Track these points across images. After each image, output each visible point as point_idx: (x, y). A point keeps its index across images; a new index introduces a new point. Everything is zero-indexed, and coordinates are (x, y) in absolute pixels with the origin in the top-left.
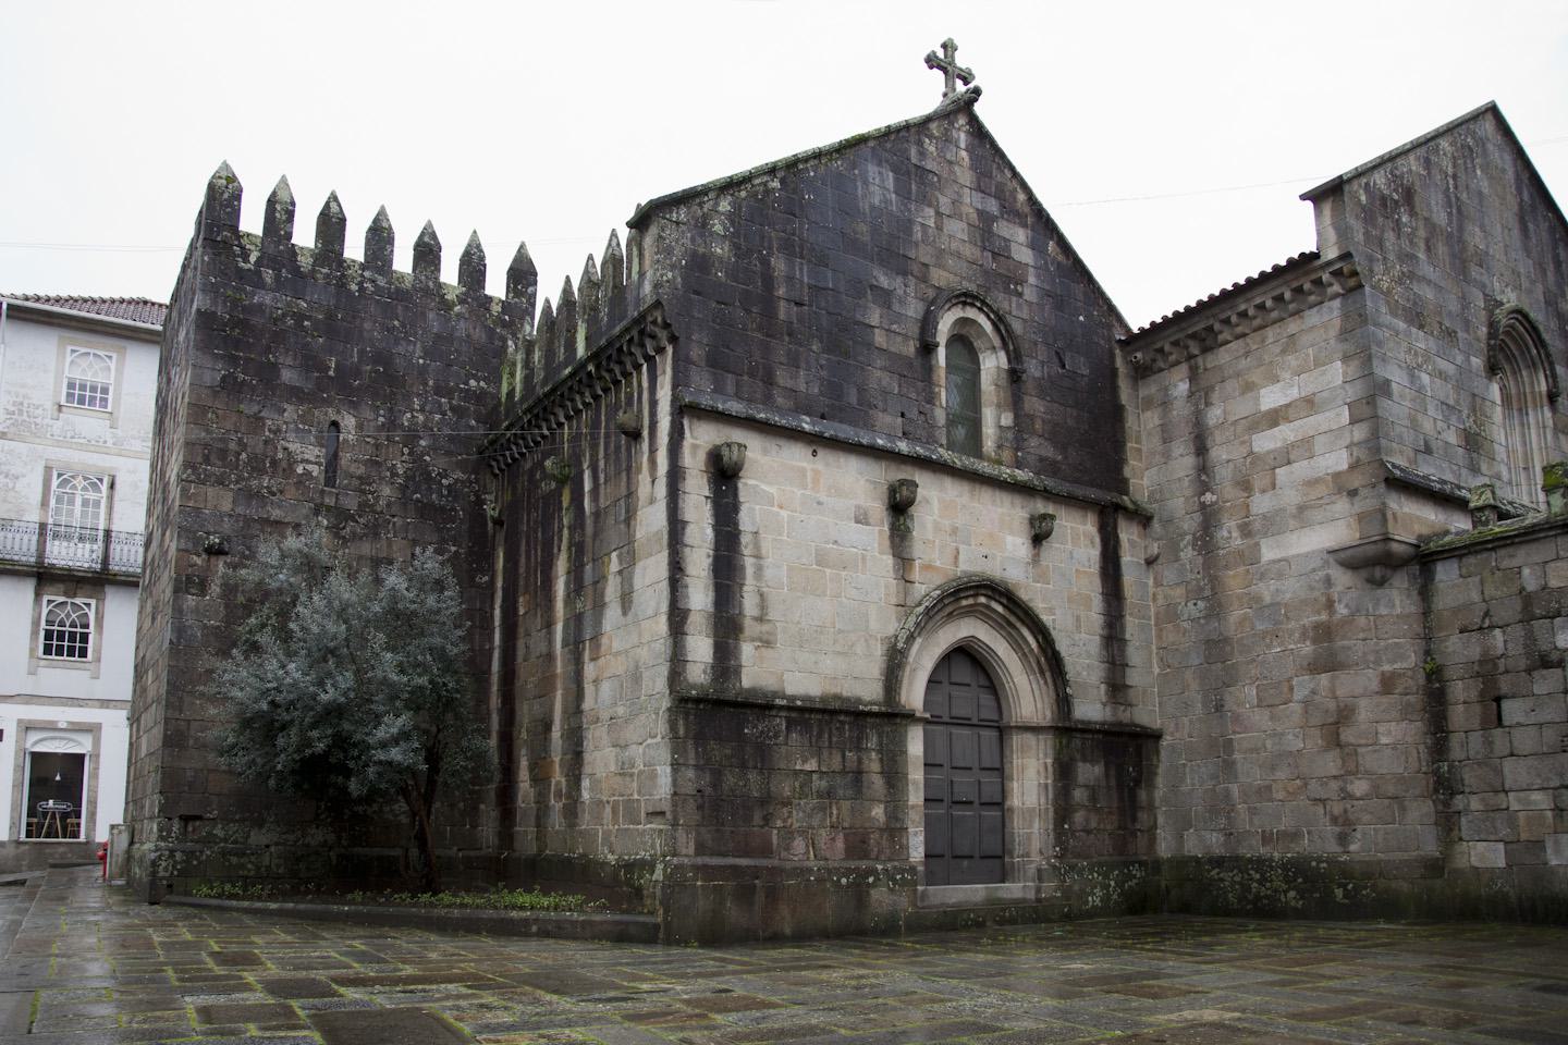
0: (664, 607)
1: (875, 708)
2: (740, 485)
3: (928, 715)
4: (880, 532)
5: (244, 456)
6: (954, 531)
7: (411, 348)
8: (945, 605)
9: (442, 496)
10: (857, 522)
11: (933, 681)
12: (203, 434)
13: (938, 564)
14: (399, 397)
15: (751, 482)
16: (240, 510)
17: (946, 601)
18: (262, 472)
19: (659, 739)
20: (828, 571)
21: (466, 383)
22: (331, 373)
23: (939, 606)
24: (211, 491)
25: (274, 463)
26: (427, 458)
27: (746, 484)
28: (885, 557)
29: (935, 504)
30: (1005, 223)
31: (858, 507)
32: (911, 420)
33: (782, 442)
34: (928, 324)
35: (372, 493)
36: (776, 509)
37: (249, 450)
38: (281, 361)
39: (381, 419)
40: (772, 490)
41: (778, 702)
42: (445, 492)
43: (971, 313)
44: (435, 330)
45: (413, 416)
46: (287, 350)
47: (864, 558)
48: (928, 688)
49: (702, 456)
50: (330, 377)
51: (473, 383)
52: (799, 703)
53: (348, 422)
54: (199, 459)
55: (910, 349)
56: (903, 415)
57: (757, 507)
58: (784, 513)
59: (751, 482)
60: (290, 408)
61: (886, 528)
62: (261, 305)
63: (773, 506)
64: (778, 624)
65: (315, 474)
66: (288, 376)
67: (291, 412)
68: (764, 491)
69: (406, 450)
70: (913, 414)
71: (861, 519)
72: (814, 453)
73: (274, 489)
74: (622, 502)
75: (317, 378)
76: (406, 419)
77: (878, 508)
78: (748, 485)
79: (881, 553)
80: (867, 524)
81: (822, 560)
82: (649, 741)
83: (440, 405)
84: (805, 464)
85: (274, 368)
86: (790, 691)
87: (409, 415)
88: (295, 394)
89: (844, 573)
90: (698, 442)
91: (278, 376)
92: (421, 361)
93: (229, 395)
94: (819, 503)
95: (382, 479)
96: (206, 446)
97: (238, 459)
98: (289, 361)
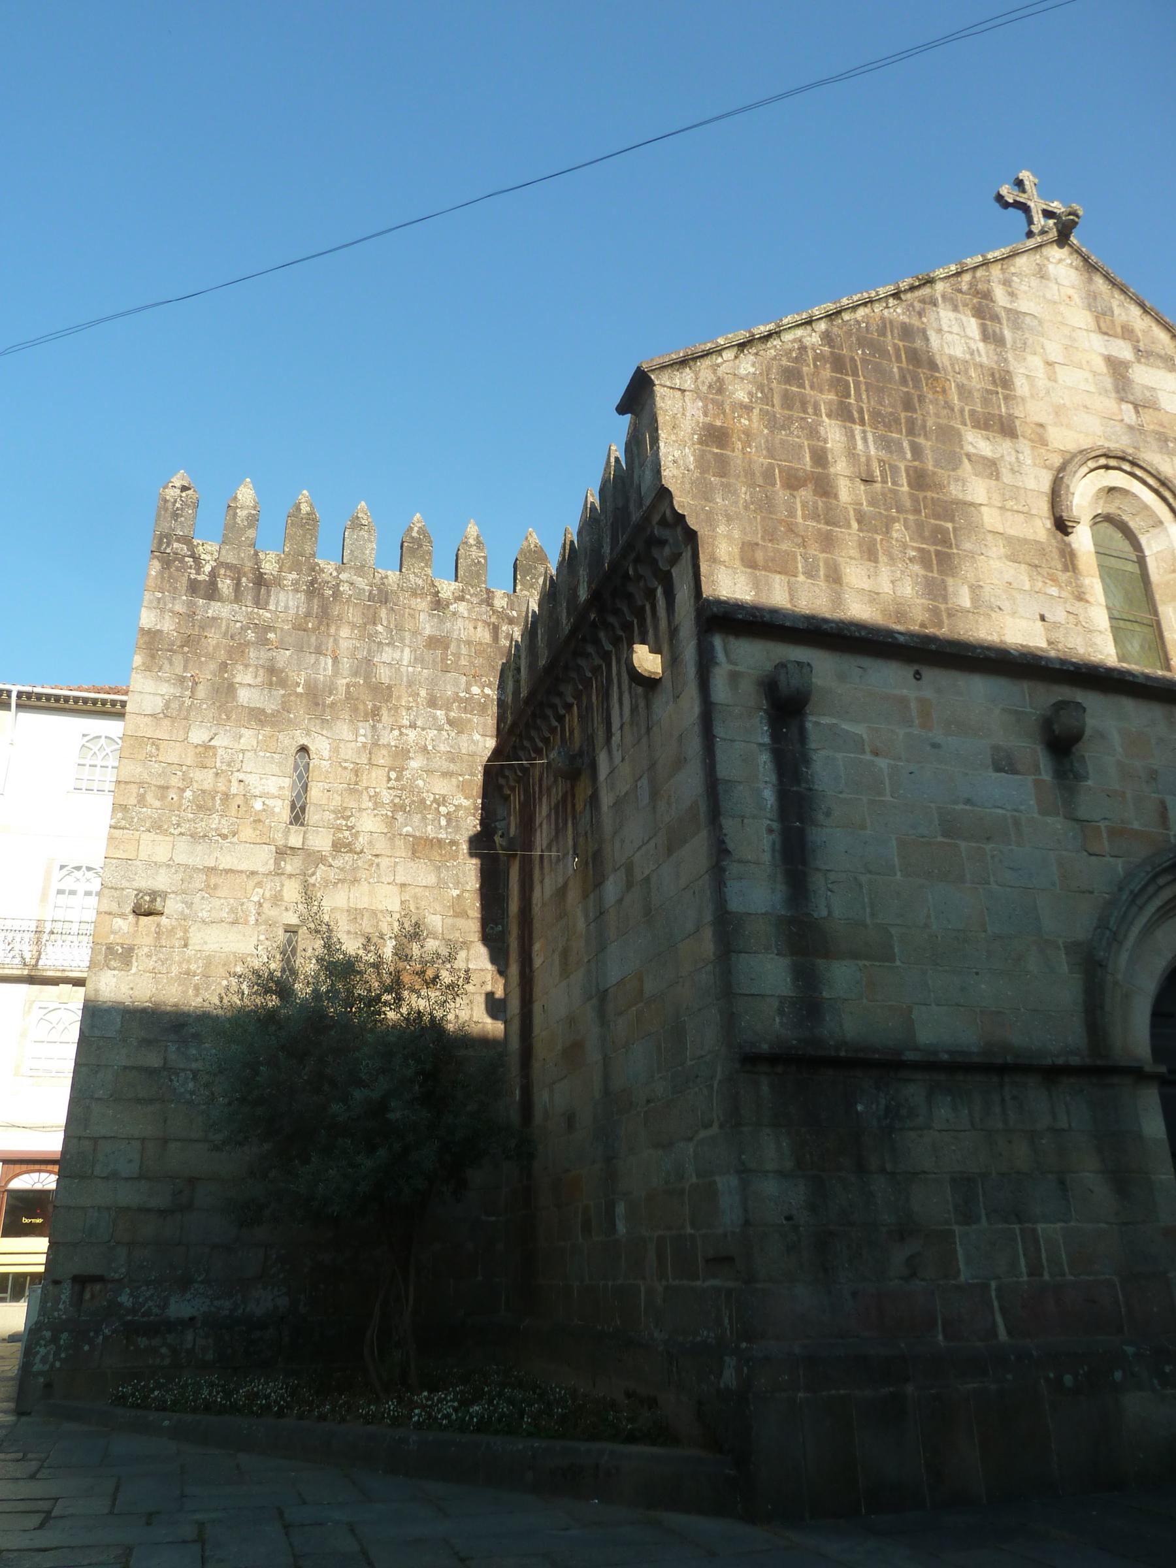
0: (708, 917)
1: (1075, 1061)
2: (809, 726)
3: (1163, 1069)
4: (1037, 783)
5: (188, 794)
6: (1153, 776)
7: (397, 655)
8: (1161, 888)
9: (441, 827)
10: (998, 769)
11: (1158, 1015)
12: (139, 770)
13: (1136, 825)
14: (384, 712)
15: (826, 720)
16: (180, 858)
17: (1161, 881)
18: (210, 811)
19: (715, 1129)
20: (963, 845)
21: (468, 691)
22: (300, 690)
23: (1151, 889)
24: (146, 837)
25: (226, 797)
26: (420, 783)
27: (817, 724)
28: (1049, 820)
29: (1116, 738)
30: (1143, 368)
31: (996, 749)
32: (1057, 625)
33: (866, 662)
34: (1057, 494)
35: (350, 828)
36: (868, 757)
37: (195, 785)
38: (237, 680)
39: (361, 739)
40: (860, 729)
41: (909, 1056)
42: (443, 822)
43: (1117, 479)
44: (428, 632)
45: (401, 734)
46: (246, 666)
47: (1017, 823)
48: (1153, 1025)
49: (748, 688)
50: (298, 695)
51: (475, 690)
52: (945, 1057)
53: (320, 746)
54: (133, 801)
55: (1041, 528)
56: (1043, 618)
57: (839, 755)
58: (883, 763)
59: (826, 720)
60: (247, 734)
61: (1047, 776)
62: (214, 619)
63: (863, 752)
64: (893, 931)
65: (277, 810)
66: (244, 696)
67: (249, 737)
68: (847, 732)
69: (393, 775)
70: (1058, 614)
71: (1004, 764)
72: (918, 676)
73: (225, 831)
74: (644, 782)
75: (283, 696)
76: (390, 738)
77: (1032, 752)
78: (817, 722)
79: (1044, 812)
80: (1014, 771)
81: (950, 828)
82: (703, 1134)
83: (435, 718)
84: (905, 692)
85: (230, 689)
86: (926, 1035)
87: (396, 732)
88: (258, 717)
89: (988, 847)
90: (737, 668)
91: (234, 698)
92: (410, 669)
93: (172, 725)
94: (935, 746)
95: (360, 810)
96: (141, 784)
97: (181, 797)
98: (248, 679)
